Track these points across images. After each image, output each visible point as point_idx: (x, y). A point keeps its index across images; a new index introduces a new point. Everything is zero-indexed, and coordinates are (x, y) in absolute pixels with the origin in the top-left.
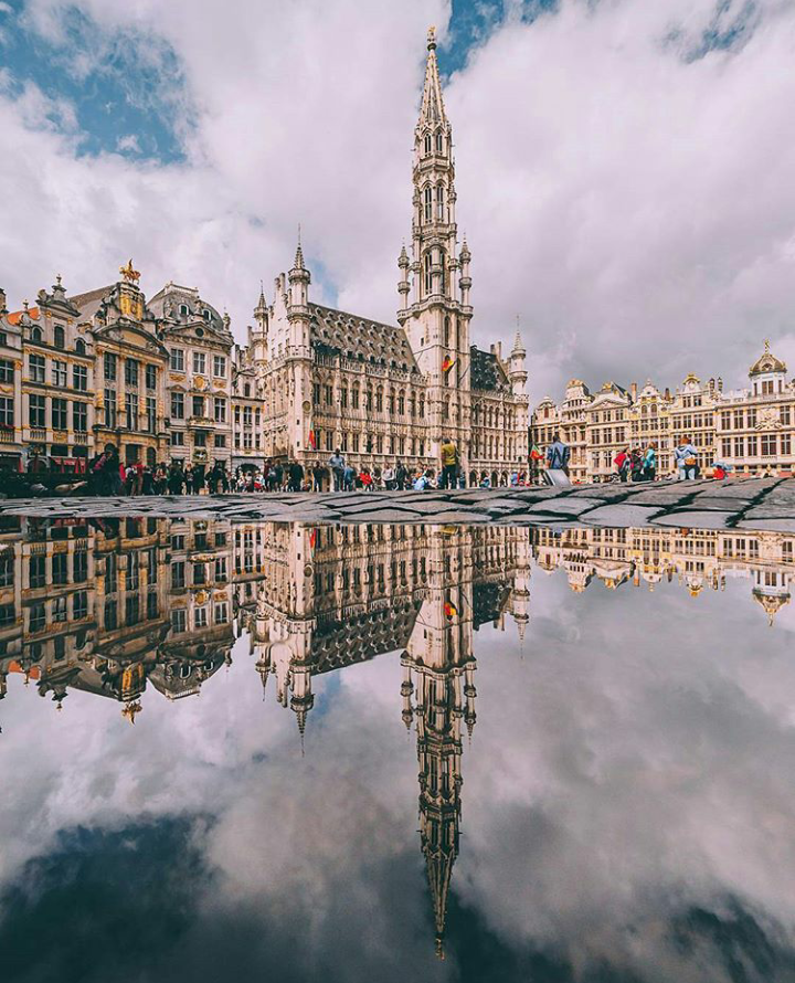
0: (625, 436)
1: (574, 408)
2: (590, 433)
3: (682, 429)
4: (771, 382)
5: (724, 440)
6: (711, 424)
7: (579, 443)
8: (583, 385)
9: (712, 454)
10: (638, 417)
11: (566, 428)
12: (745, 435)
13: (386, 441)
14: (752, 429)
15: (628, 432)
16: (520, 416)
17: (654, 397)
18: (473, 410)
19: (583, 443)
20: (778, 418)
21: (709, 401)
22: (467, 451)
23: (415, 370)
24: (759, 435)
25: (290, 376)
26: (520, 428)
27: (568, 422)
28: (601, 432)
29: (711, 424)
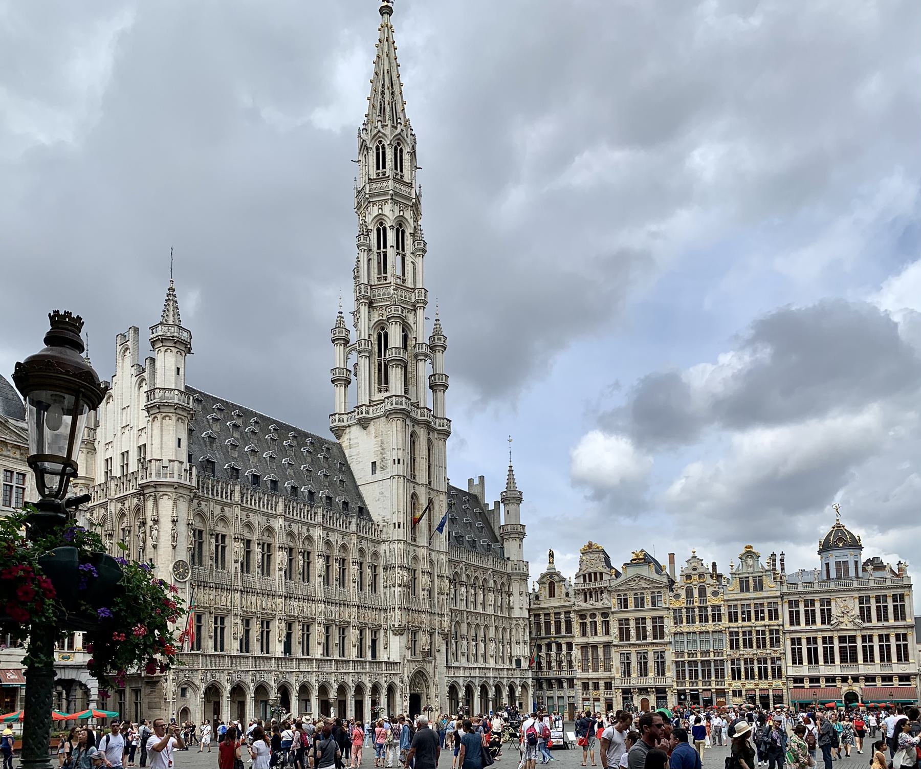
2: (616, 624)
4: (846, 563)
5: (793, 640)
7: (600, 638)
9: (779, 659)
10: (681, 603)
13: (317, 633)
15: (669, 626)
18: (450, 581)
19: (606, 639)
23: (363, 511)
25: (149, 513)
26: (516, 613)
27: (584, 605)
28: (632, 624)
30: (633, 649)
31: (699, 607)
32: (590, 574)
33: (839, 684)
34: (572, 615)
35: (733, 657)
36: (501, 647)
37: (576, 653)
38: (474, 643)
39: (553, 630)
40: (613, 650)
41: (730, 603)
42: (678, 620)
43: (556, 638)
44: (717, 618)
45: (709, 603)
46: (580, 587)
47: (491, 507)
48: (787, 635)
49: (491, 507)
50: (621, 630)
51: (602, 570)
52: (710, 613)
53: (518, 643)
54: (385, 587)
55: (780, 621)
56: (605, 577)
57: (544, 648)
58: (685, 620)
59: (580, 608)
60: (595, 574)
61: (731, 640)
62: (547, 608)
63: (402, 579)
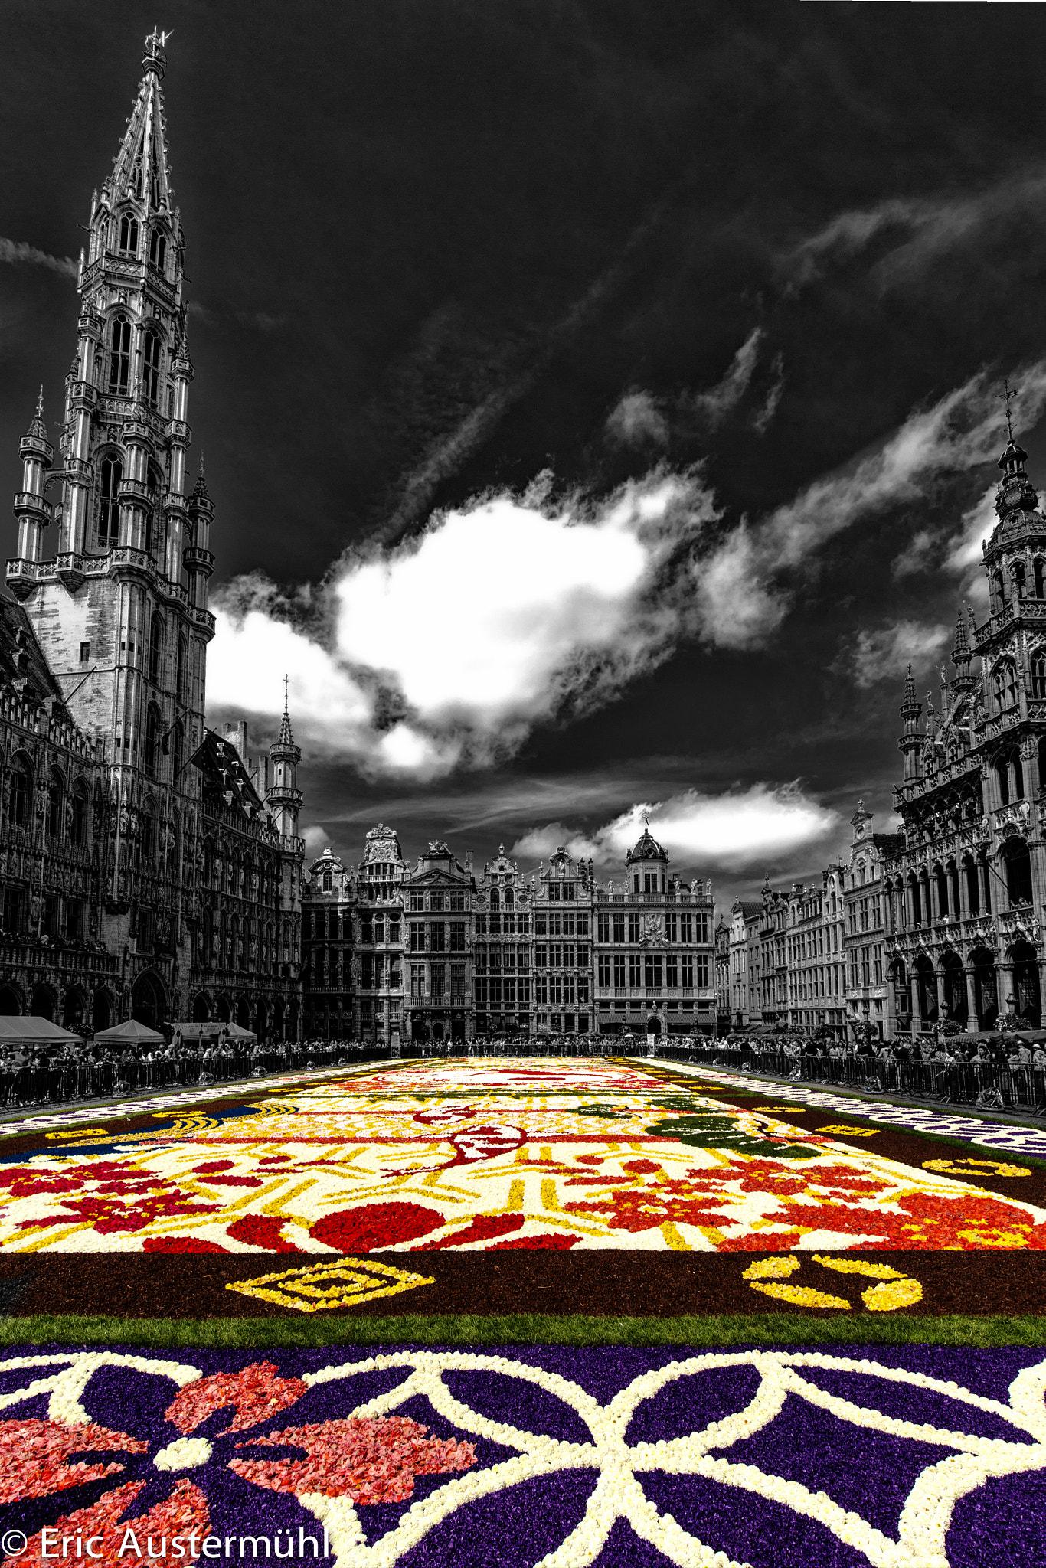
5: (601, 958)
10: (485, 908)
12: (627, 953)
15: (471, 934)
17: (509, 876)
20: (663, 930)
24: (643, 954)
26: (286, 905)
29: (586, 933)
32: (378, 865)
33: (642, 1009)
37: (355, 962)
39: (327, 934)
42: (480, 928)
43: (330, 943)
50: (413, 937)
52: (516, 922)
54: (97, 837)
60: (385, 865)
61: (538, 956)
62: (321, 905)
63: (129, 827)
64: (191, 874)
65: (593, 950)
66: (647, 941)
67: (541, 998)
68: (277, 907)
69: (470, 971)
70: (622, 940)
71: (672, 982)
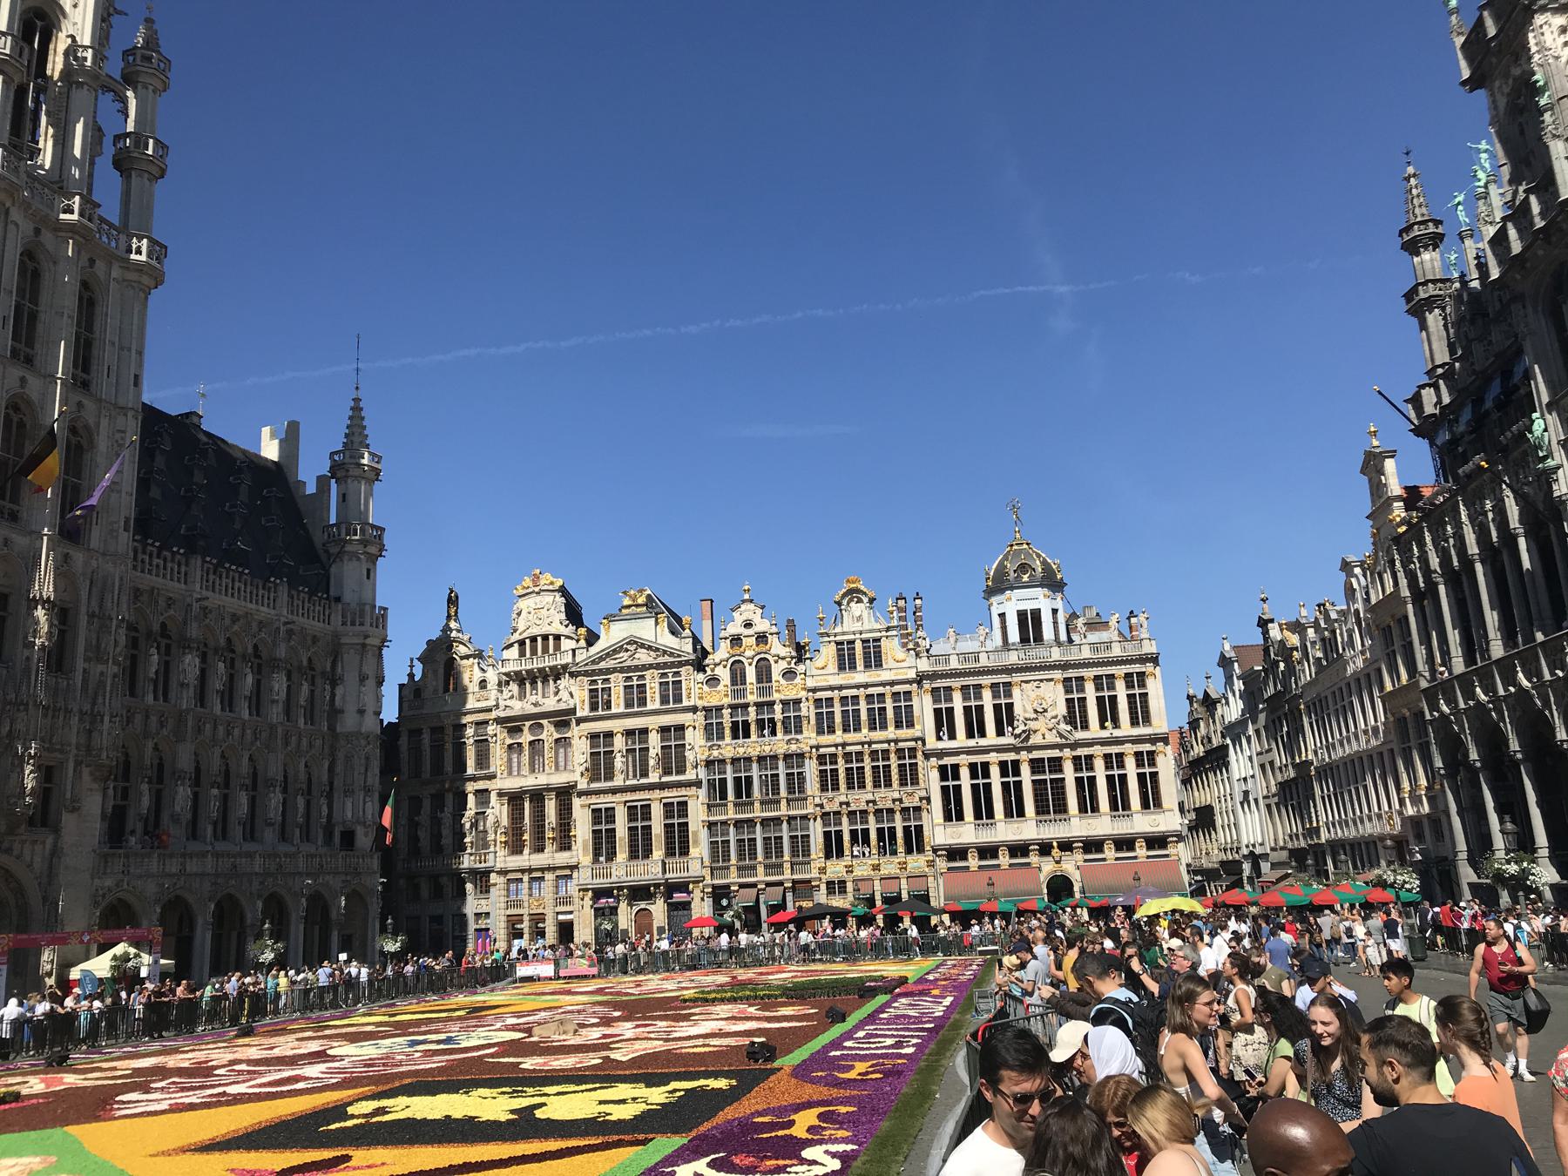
0: (689, 755)
1: (537, 664)
3: (839, 736)
5: (943, 770)
6: (911, 725)
8: (563, 591)
9: (918, 809)
10: (720, 696)
11: (513, 725)
14: (1007, 740)
15: (696, 744)
16: (351, 678)
17: (762, 638)
20: (1062, 709)
21: (901, 654)
22: (94, 804)
24: (1024, 756)
26: (348, 722)
27: (518, 707)
28: (619, 743)
29: (911, 725)
30: (619, 798)
31: (758, 705)
32: (533, 639)
34: (491, 729)
35: (827, 809)
36: (301, 801)
38: (215, 791)
40: (577, 802)
41: (819, 695)
42: (713, 732)
44: (794, 725)
45: (776, 696)
46: (511, 667)
47: (311, 489)
48: (933, 760)
49: (311, 489)
51: (562, 630)
52: (778, 716)
53: (348, 792)
55: (916, 732)
56: (567, 644)
57: (427, 804)
58: (727, 732)
59: (508, 713)
60: (545, 638)
64: (101, 684)
65: (927, 756)
66: (1028, 734)
67: (833, 847)
68: (332, 728)
69: (697, 815)
70: (983, 734)
71: (1088, 805)
